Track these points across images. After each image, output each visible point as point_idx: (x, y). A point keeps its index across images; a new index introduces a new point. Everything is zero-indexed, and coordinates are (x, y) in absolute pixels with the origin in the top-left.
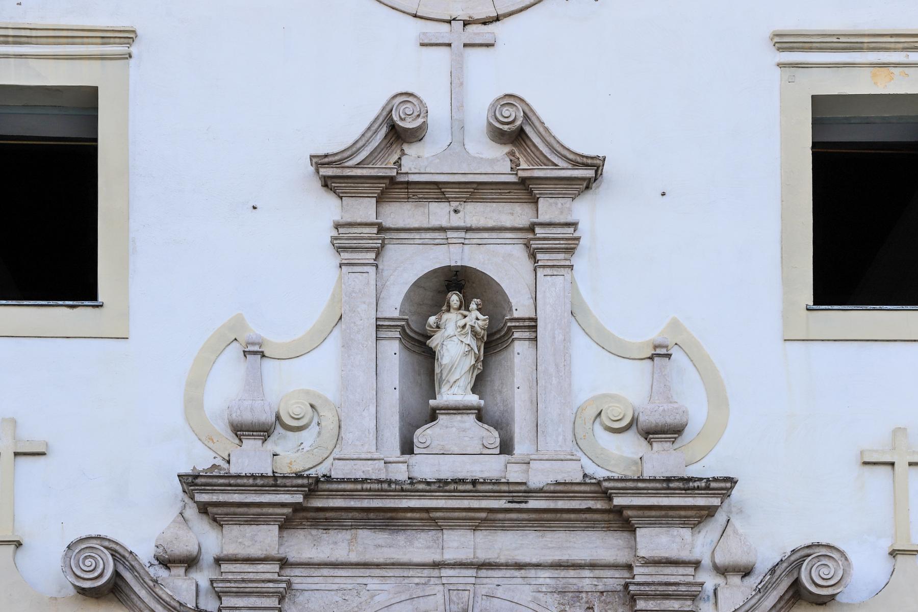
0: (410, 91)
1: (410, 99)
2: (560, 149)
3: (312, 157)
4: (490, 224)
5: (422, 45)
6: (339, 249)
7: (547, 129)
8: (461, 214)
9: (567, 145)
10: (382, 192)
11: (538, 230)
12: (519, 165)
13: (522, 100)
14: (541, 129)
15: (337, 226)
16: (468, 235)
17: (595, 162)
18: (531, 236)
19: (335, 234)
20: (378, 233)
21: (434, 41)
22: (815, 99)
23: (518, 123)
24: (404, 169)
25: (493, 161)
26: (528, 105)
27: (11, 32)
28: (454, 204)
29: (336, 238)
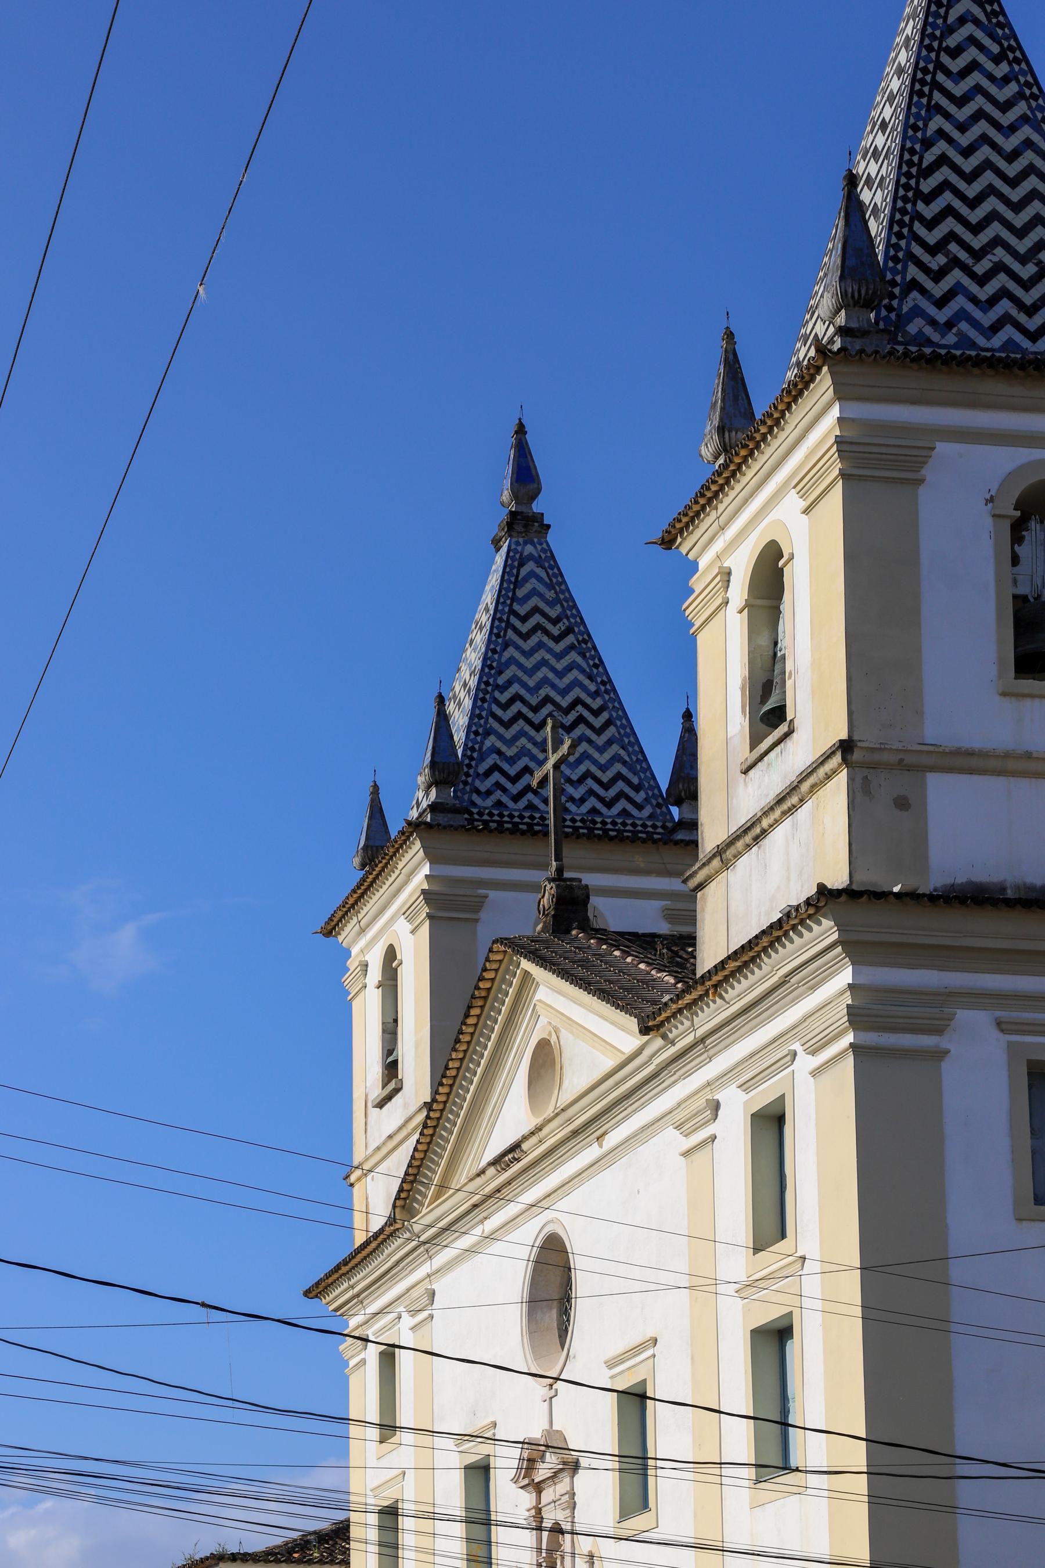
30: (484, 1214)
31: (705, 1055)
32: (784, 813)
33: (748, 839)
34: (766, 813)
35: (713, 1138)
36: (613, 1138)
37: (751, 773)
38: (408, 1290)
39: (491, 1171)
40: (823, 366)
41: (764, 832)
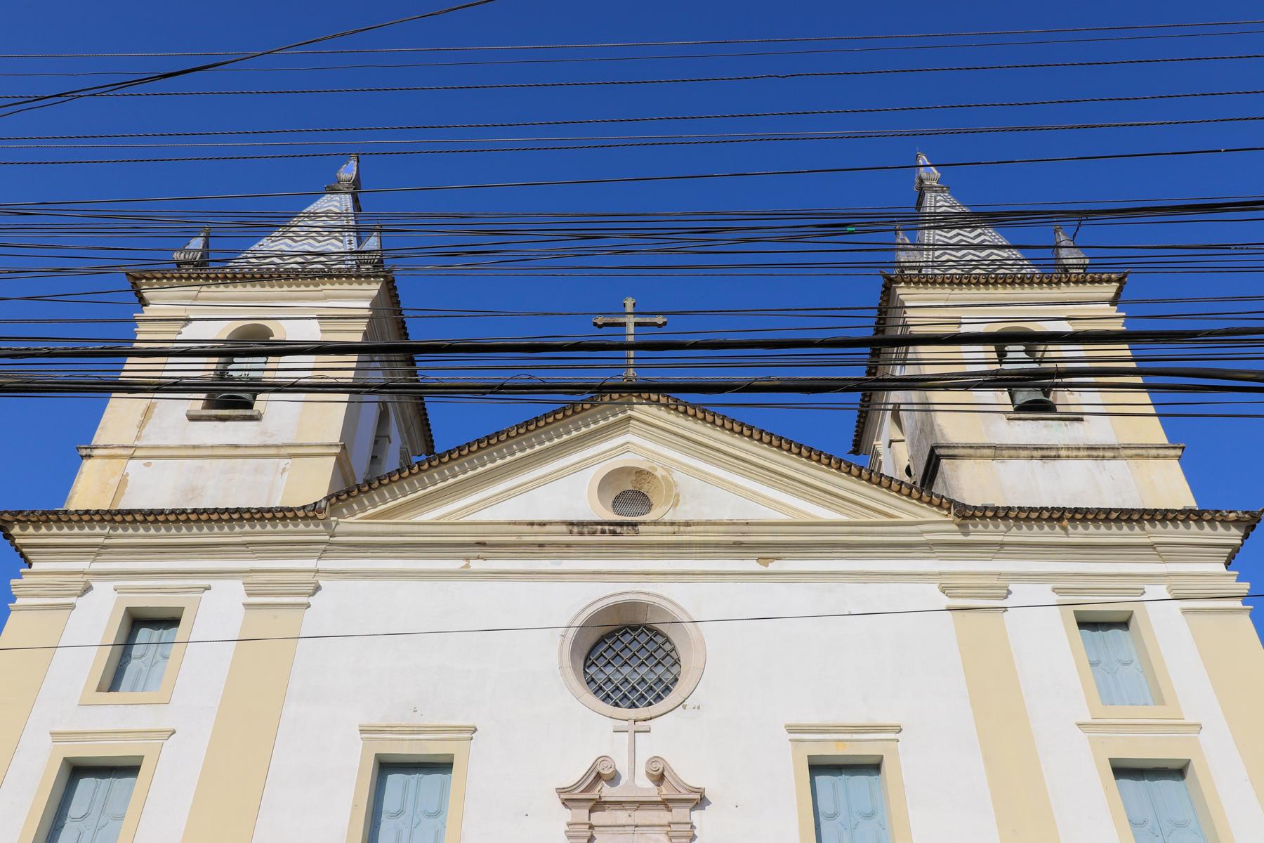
0: (607, 755)
1: (607, 759)
2: (682, 784)
3: (557, 789)
4: (648, 823)
5: (614, 731)
6: (569, 837)
7: (675, 774)
8: (633, 818)
9: (685, 781)
10: (592, 807)
11: (672, 826)
12: (661, 792)
13: (663, 759)
14: (673, 774)
15: (569, 824)
16: (636, 829)
17: (700, 790)
18: (669, 829)
19: (567, 829)
20: (589, 828)
21: (620, 730)
22: (808, 756)
23: (661, 770)
24: (602, 795)
25: (648, 790)
26: (666, 762)
27: (416, 729)
28: (629, 812)
29: (568, 832)
30: (481, 555)
31: (991, 555)
32: (1089, 456)
33: (1035, 453)
34: (1068, 448)
35: (1005, 609)
36: (774, 566)
37: (1012, 423)
38: (252, 571)
39: (564, 528)
40: (1115, 282)
41: (1058, 457)
